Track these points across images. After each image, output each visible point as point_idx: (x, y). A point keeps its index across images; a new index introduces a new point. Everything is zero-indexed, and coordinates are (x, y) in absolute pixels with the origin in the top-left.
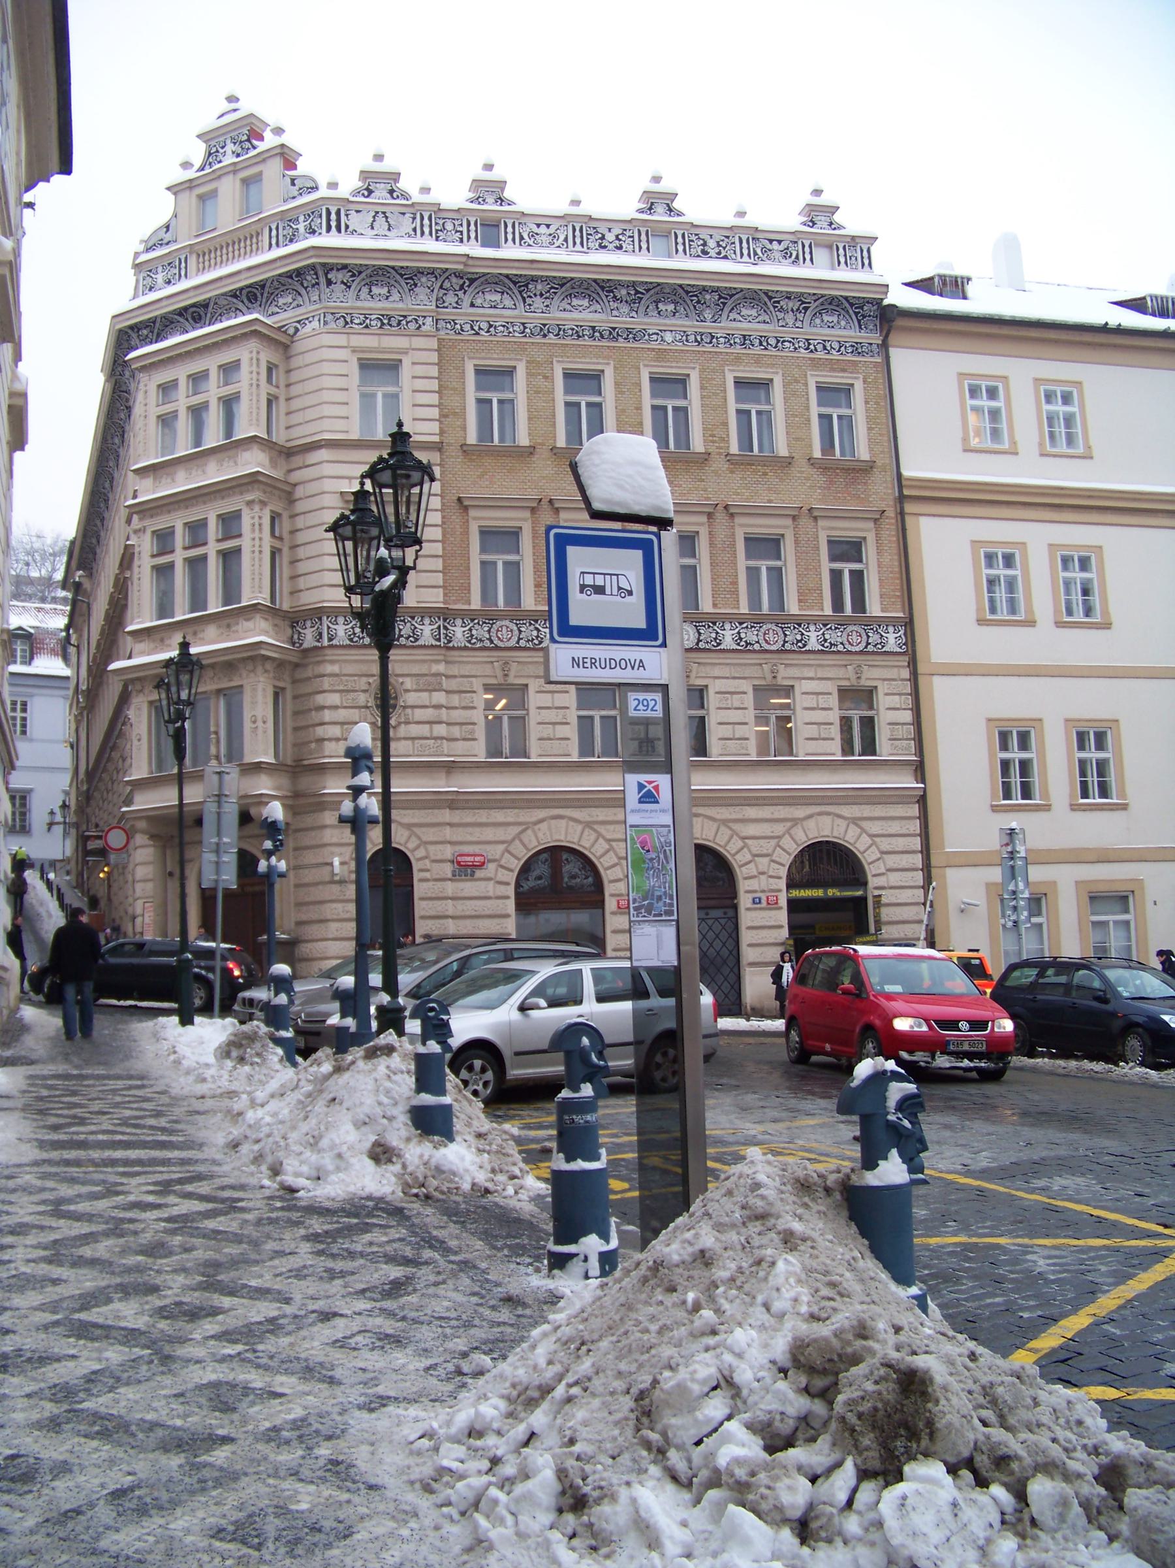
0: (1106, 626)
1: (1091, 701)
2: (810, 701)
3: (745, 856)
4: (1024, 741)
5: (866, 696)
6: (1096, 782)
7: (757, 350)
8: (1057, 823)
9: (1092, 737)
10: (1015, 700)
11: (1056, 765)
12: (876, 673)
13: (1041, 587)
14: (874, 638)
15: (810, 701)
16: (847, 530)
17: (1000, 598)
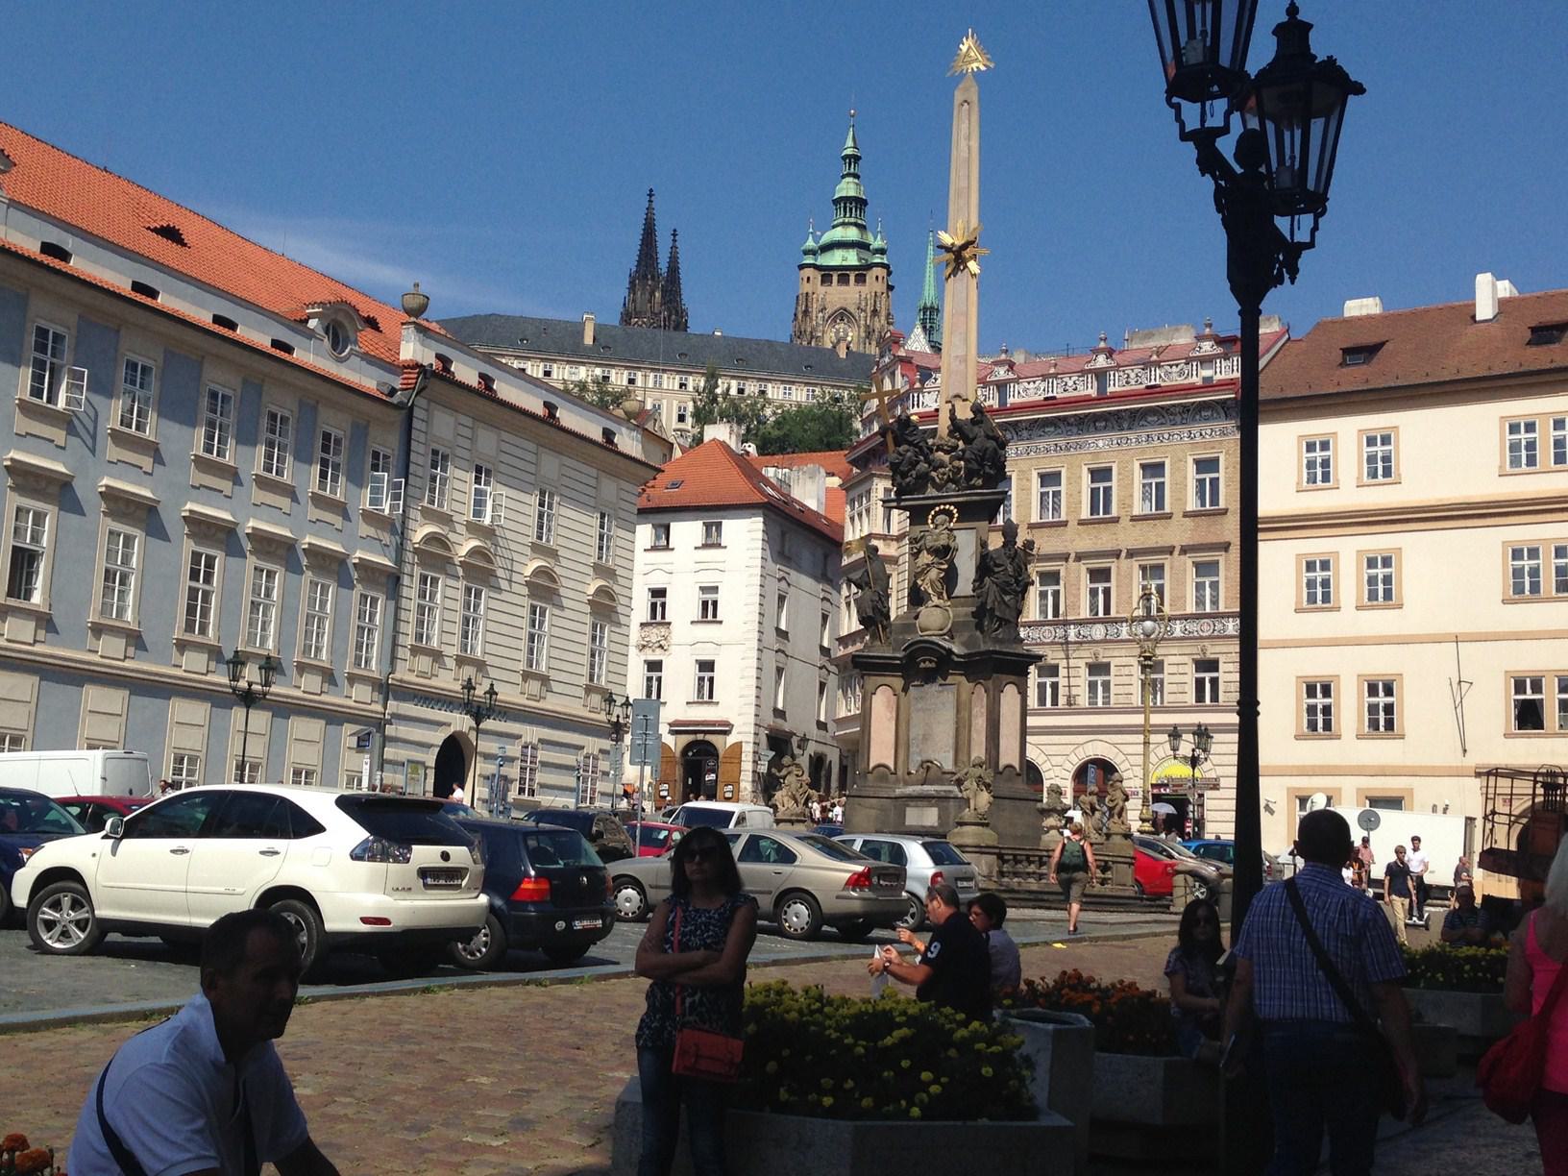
0: (1400, 606)
1: (1380, 662)
2: (1174, 669)
3: (1126, 765)
4: (1327, 691)
5: (1211, 665)
6: (1383, 720)
7: (1156, 443)
8: (1351, 744)
9: (1382, 688)
10: (1318, 664)
11: (1349, 707)
12: (1218, 649)
13: (1348, 582)
14: (1219, 626)
15: (1174, 669)
16: (1205, 557)
17: (1319, 593)
